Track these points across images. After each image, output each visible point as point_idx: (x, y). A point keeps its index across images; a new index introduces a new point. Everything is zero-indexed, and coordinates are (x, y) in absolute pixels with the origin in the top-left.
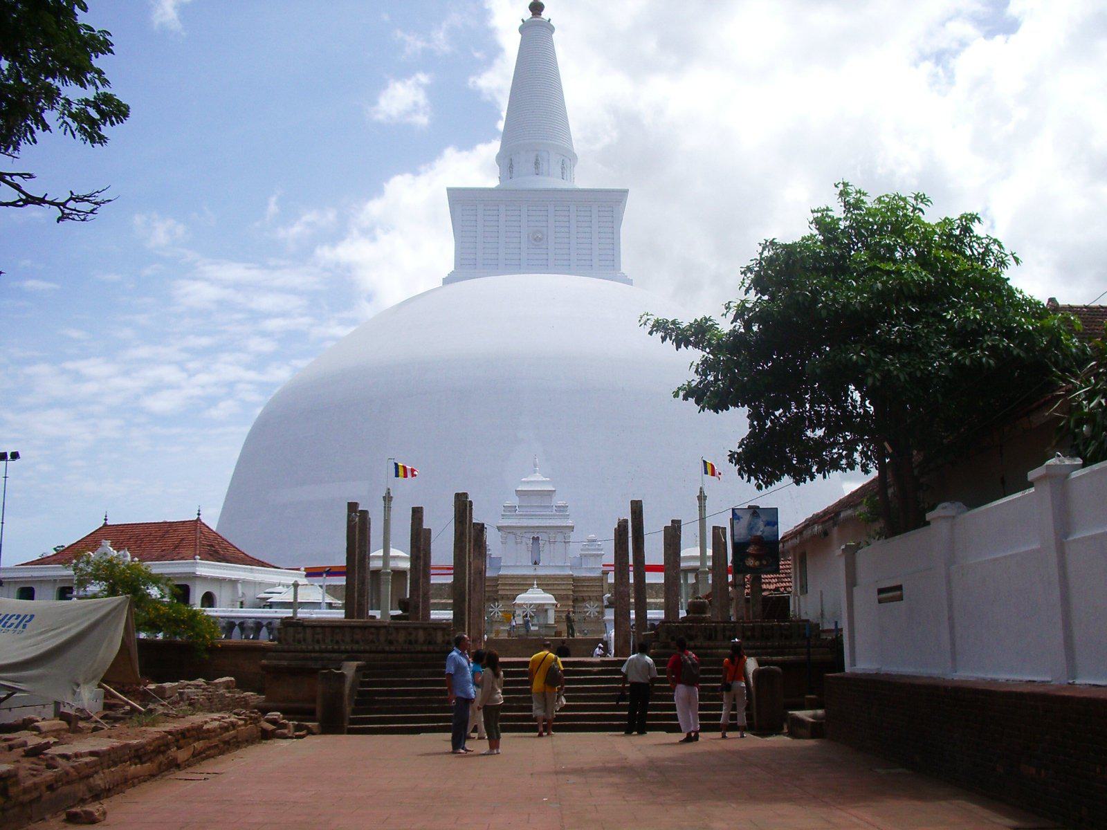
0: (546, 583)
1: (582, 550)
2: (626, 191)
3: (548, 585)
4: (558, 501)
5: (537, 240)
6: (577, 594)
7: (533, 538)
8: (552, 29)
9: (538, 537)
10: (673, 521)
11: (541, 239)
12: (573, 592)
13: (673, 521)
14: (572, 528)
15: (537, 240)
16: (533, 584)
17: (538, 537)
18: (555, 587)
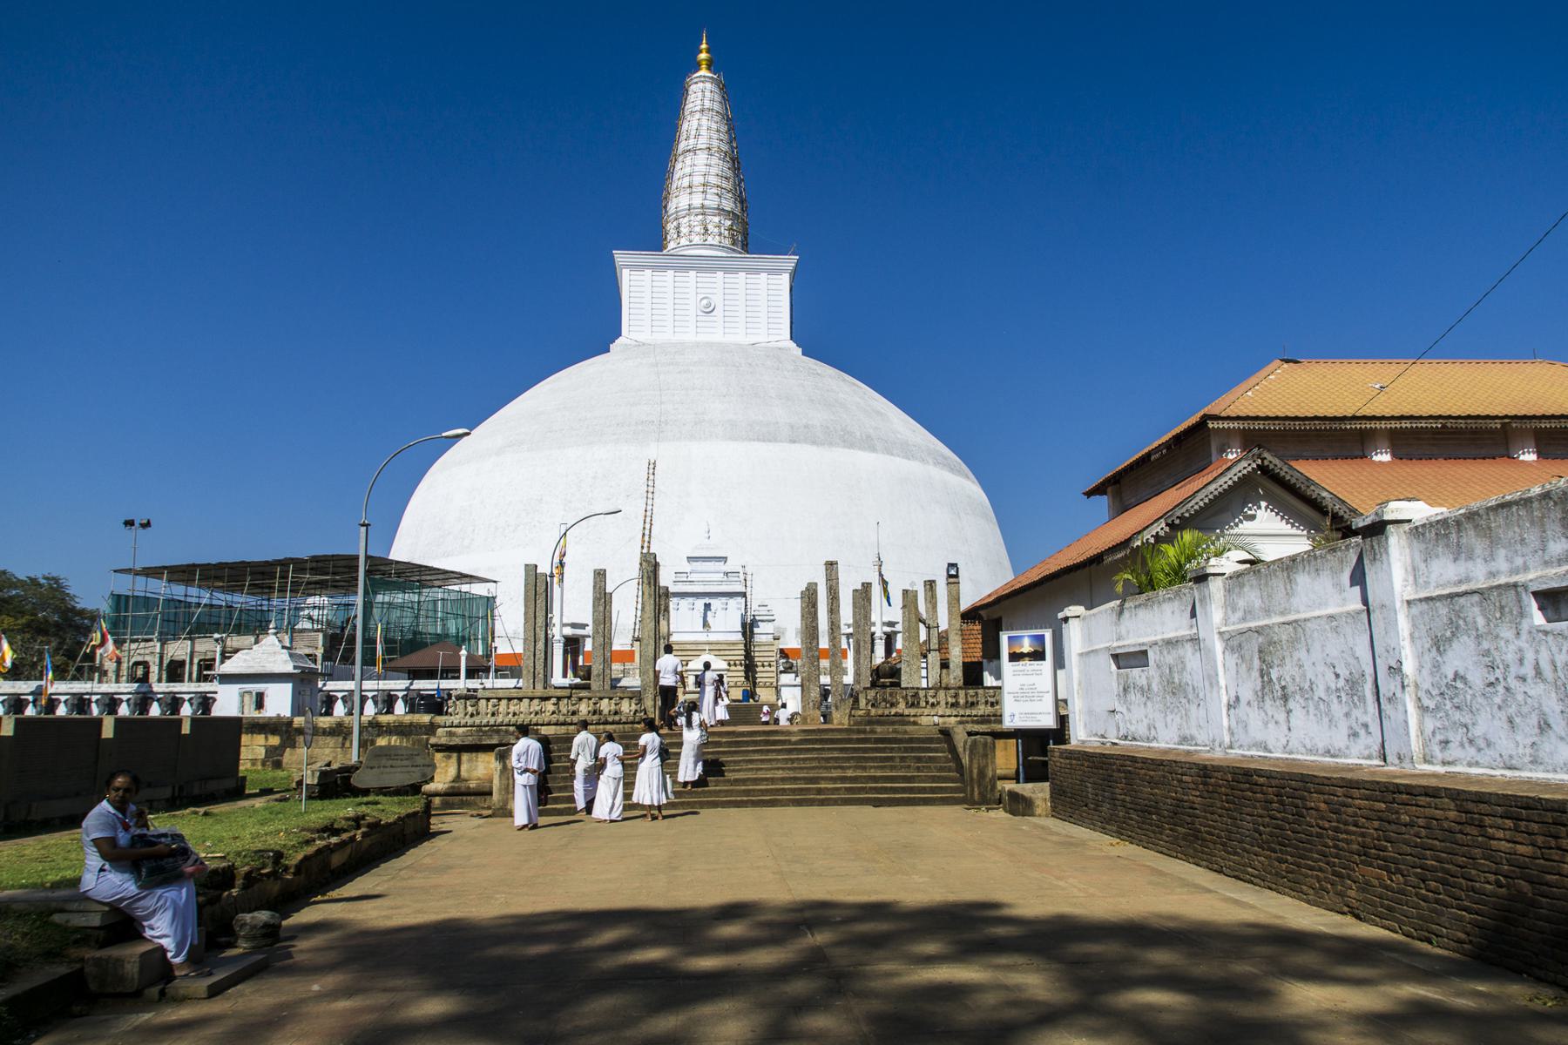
7: (705, 604)
9: (710, 604)
10: (863, 584)
13: (863, 584)
17: (710, 604)
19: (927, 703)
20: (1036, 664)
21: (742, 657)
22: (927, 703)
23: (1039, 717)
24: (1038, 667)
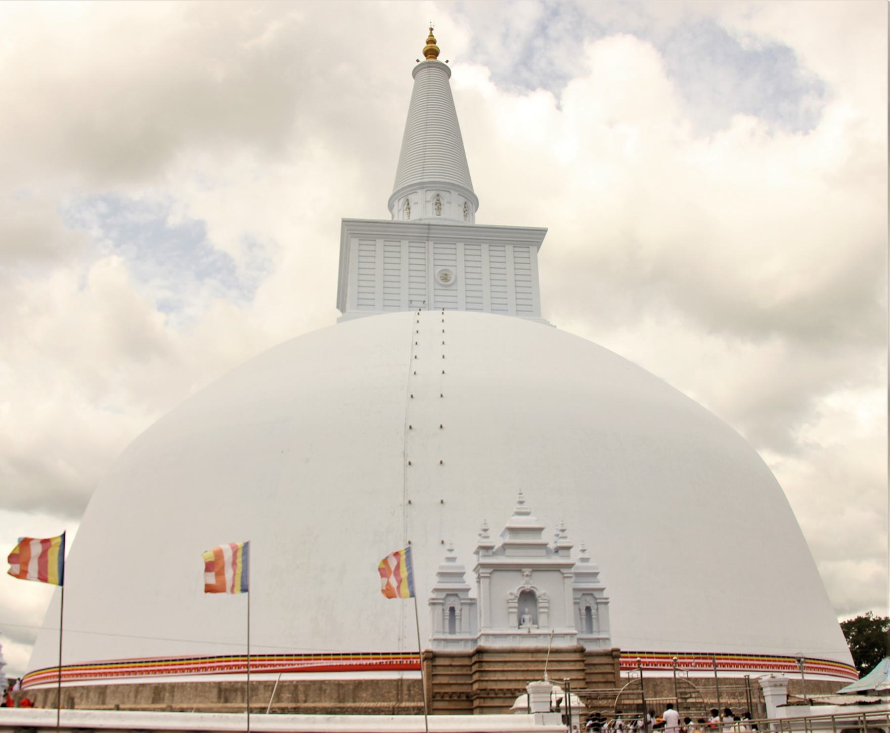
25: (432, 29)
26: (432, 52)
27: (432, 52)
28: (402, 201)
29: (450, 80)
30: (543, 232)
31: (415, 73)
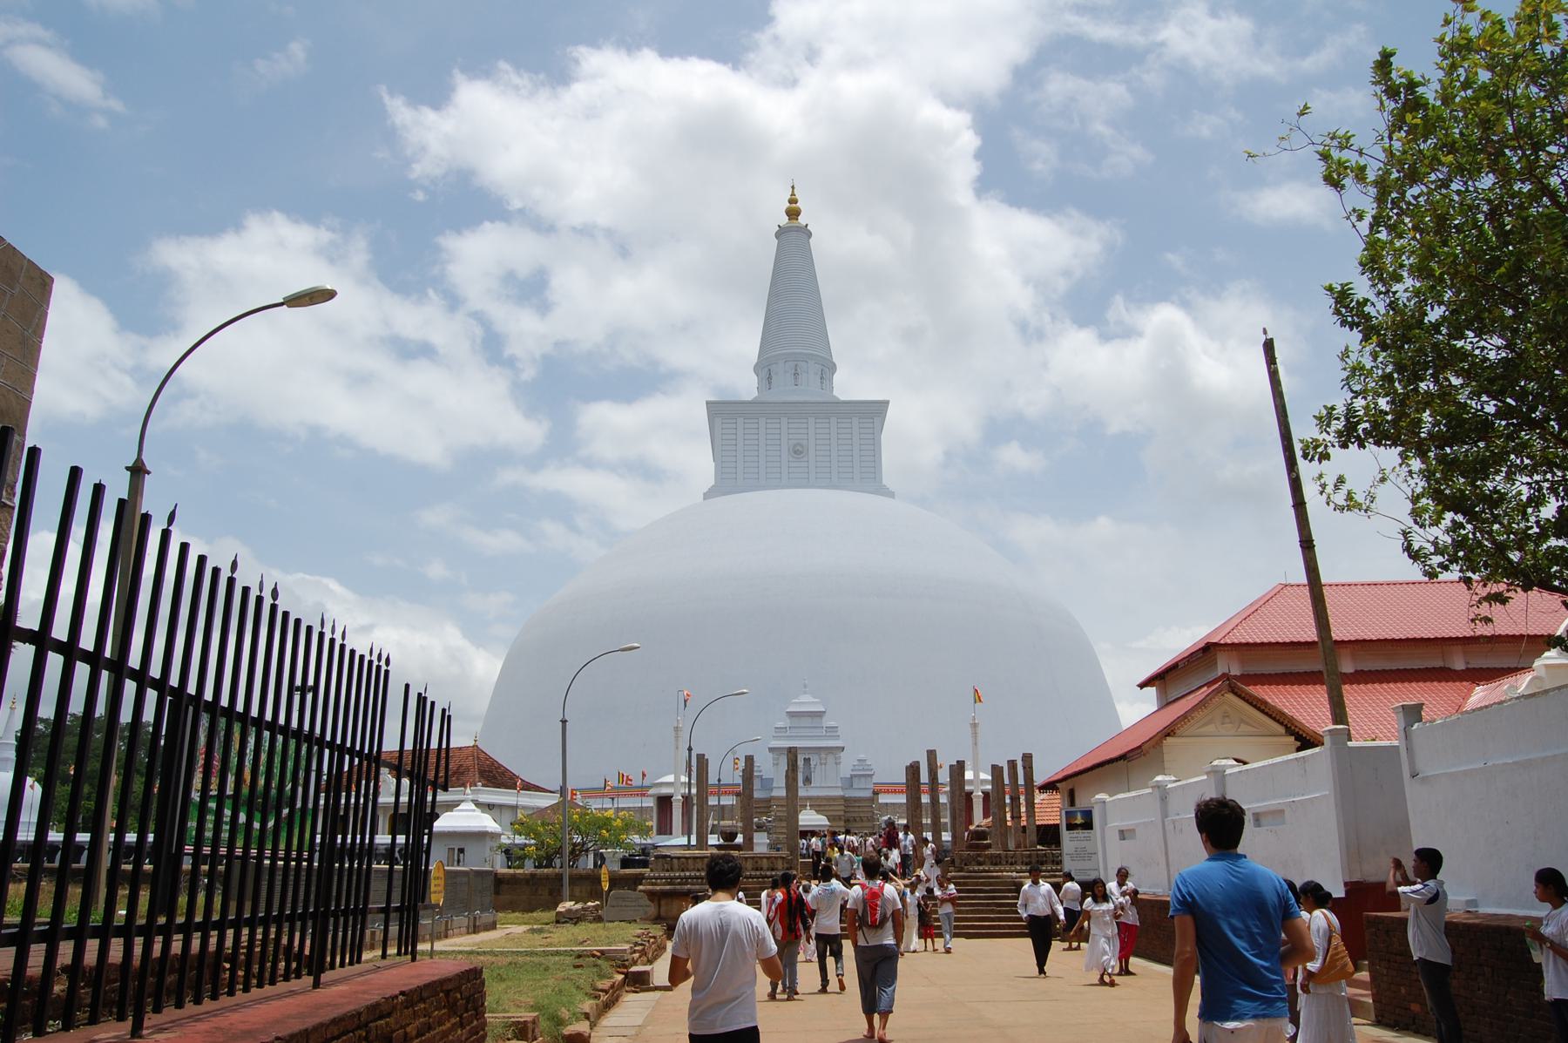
0: (819, 805)
1: (852, 770)
2: (887, 402)
3: (819, 806)
4: (828, 722)
5: (798, 451)
6: (849, 815)
8: (810, 235)
9: (809, 759)
10: (958, 762)
11: (801, 453)
12: (845, 812)
13: (958, 762)
14: (843, 749)
15: (798, 451)
16: (806, 806)
17: (809, 759)
18: (827, 808)
19: (1007, 862)
20: (1087, 833)
21: (842, 813)
22: (1007, 862)
23: (1089, 872)
24: (1087, 835)
25: (793, 187)
26: (793, 213)
27: (793, 213)
28: (766, 369)
29: (811, 240)
30: (887, 402)
31: (778, 235)
